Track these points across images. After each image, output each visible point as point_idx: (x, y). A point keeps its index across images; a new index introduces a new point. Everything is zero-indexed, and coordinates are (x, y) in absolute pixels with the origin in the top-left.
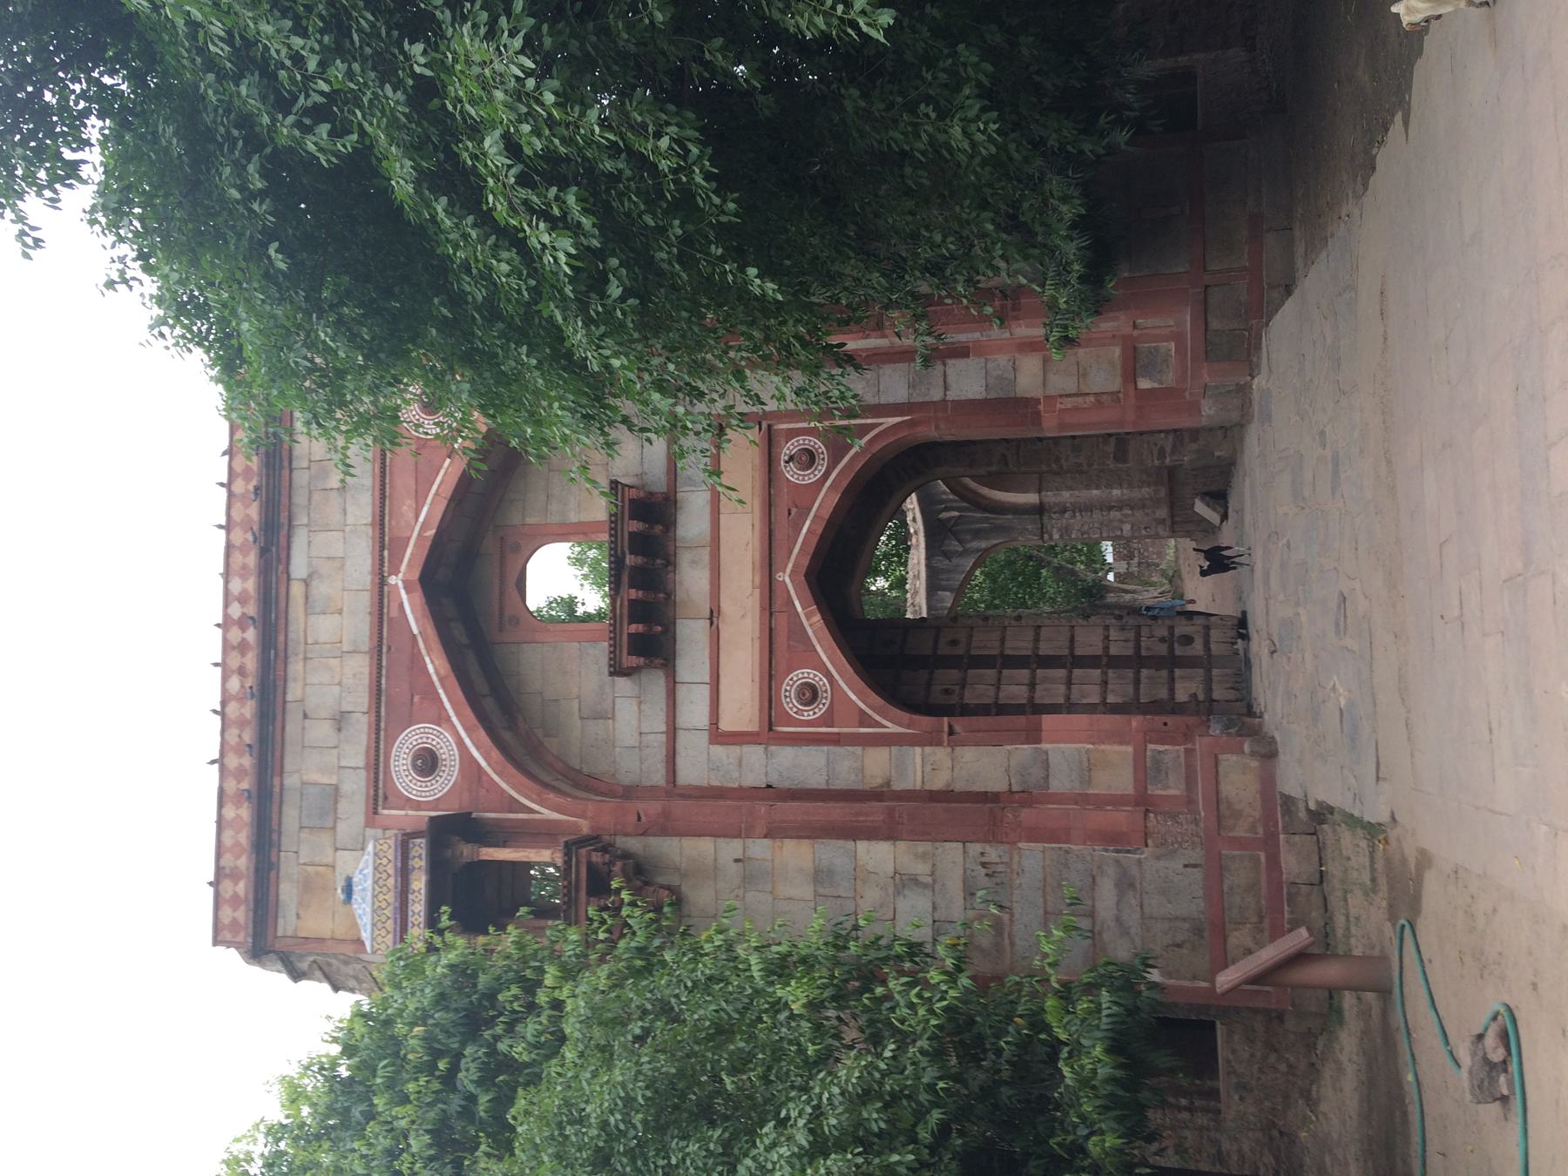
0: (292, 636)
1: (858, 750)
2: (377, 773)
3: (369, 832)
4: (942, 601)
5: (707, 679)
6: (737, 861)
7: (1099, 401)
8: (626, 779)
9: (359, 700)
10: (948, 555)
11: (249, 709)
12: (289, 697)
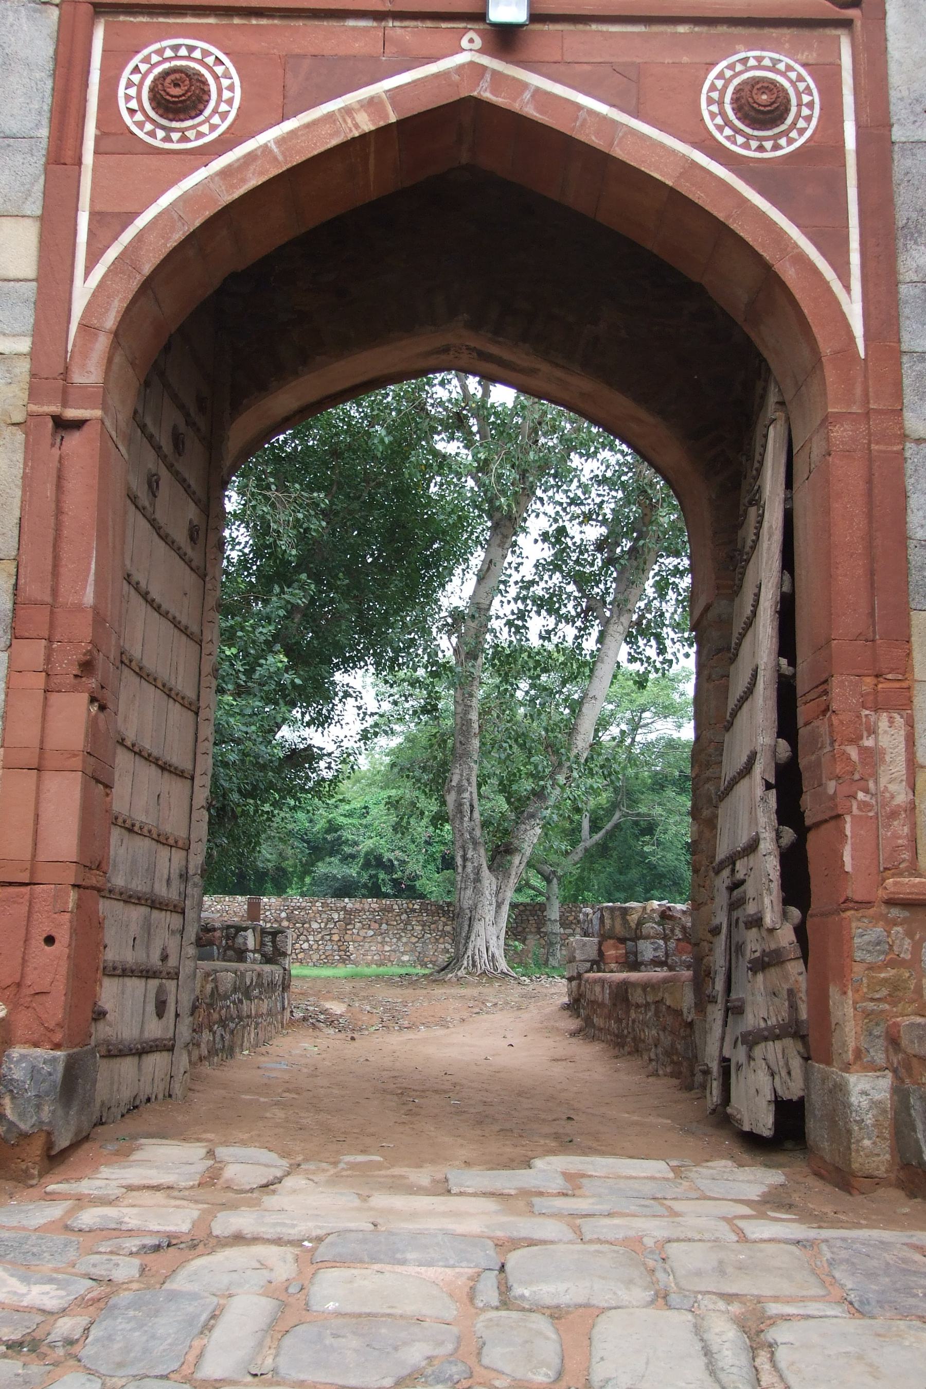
1: (34, 207)
7: (894, 815)
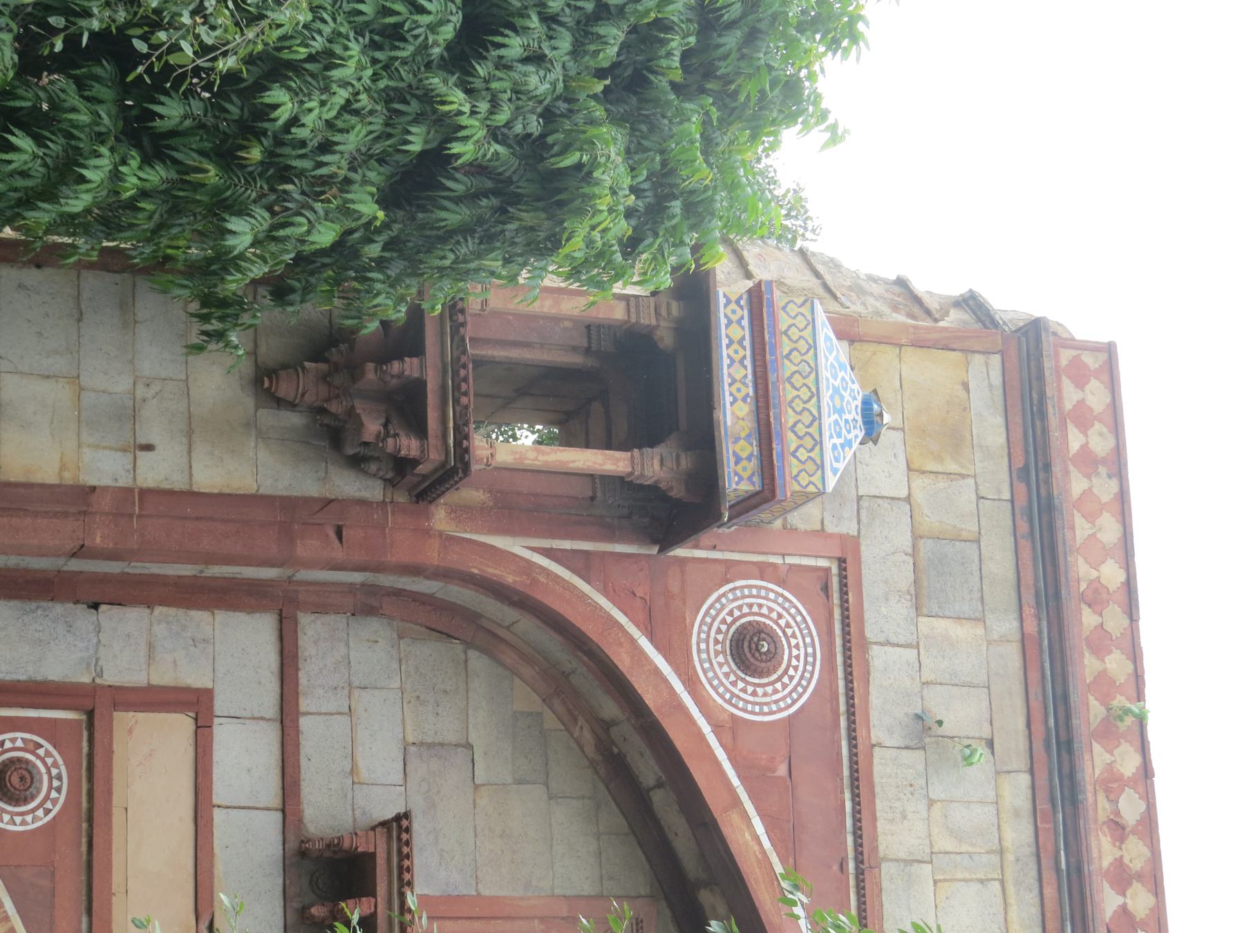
0: (1032, 897)
2: (846, 633)
3: (849, 528)
5: (218, 815)
6: (149, 448)
8: (374, 626)
9: (890, 769)
11: (1096, 760)
12: (1024, 779)
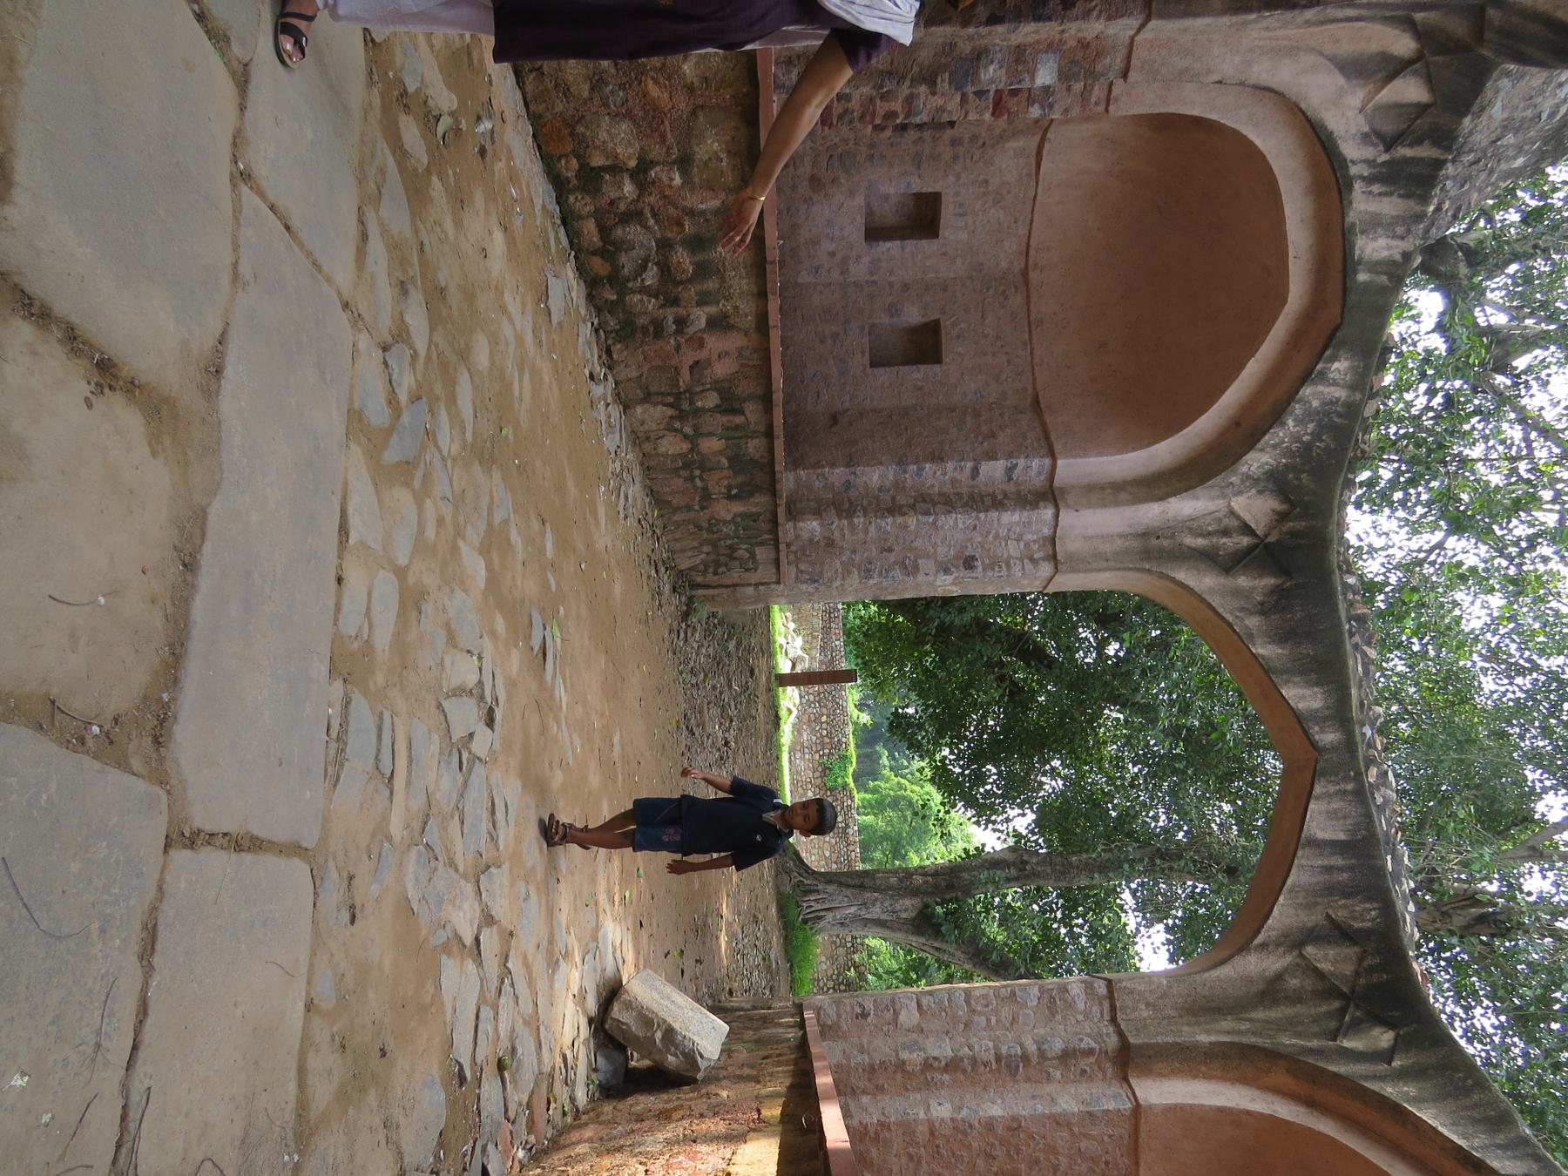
4: (1332, 815)
10: (1340, 933)
